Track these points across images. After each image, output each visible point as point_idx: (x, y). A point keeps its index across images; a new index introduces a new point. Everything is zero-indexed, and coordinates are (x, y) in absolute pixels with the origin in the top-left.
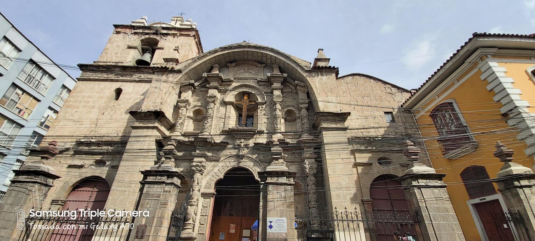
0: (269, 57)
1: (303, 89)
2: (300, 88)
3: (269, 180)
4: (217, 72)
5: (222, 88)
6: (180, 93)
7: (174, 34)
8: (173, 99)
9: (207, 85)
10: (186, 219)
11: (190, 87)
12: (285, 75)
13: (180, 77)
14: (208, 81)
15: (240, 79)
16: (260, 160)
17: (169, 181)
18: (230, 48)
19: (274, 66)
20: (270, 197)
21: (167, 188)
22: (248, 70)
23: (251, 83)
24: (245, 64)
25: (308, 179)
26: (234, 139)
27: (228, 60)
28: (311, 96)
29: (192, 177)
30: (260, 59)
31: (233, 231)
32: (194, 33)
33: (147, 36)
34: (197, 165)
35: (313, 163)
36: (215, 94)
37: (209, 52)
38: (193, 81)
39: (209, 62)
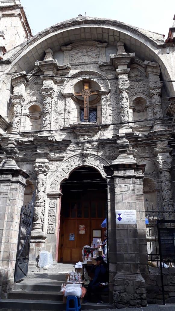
0: (111, 33)
1: (155, 71)
2: (151, 70)
3: (116, 173)
4: (51, 59)
5: (59, 79)
6: (12, 88)
8: (6, 96)
10: (34, 220)
11: (22, 79)
12: (132, 54)
13: (9, 69)
14: (41, 71)
15: (77, 65)
16: (106, 158)
17: (14, 179)
18: (63, 26)
19: (118, 44)
20: (117, 190)
21: (13, 186)
22: (87, 52)
24: (83, 45)
25: (162, 175)
26: (77, 136)
27: (62, 42)
28: (164, 78)
29: (36, 178)
30: (100, 37)
31: (82, 232)
32: (18, 11)
34: (40, 166)
35: (167, 157)
36: (51, 86)
37: (40, 35)
38: (24, 72)
39: (40, 47)
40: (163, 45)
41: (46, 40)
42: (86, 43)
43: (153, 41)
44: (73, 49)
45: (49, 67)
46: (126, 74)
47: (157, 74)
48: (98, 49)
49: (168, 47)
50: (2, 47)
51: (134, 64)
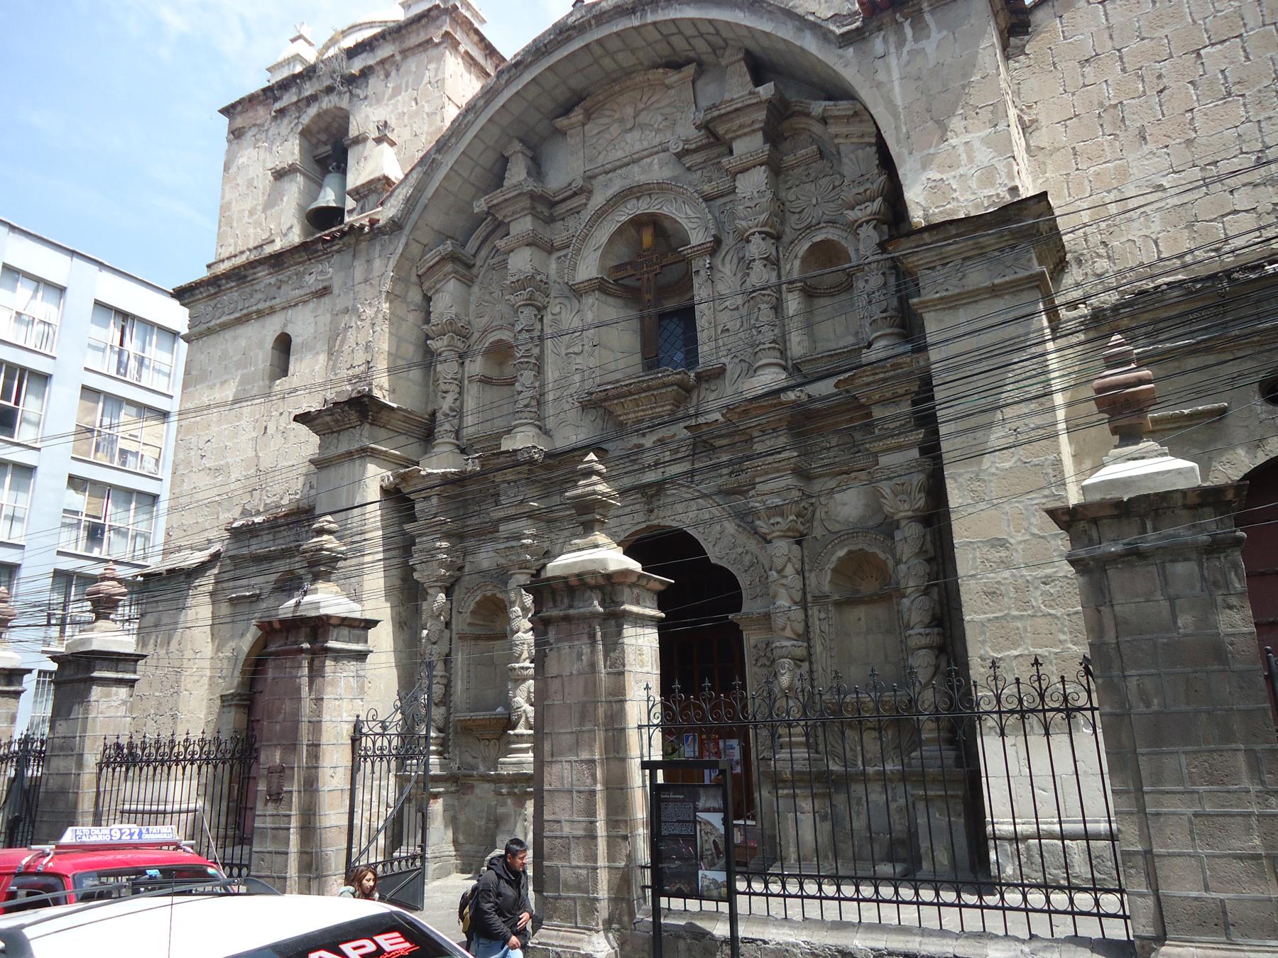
0: (690, 31)
1: (855, 129)
2: (844, 130)
7: (382, 62)
9: (500, 244)
23: (657, 171)
24: (621, 92)
30: (663, 49)
33: (312, 111)
40: (857, 29)
41: (490, 120)
42: (628, 83)
43: (820, 27)
44: (594, 116)
45: (518, 207)
46: (761, 165)
47: (867, 140)
48: (672, 92)
49: (880, 29)
50: (379, 179)
51: (788, 118)
